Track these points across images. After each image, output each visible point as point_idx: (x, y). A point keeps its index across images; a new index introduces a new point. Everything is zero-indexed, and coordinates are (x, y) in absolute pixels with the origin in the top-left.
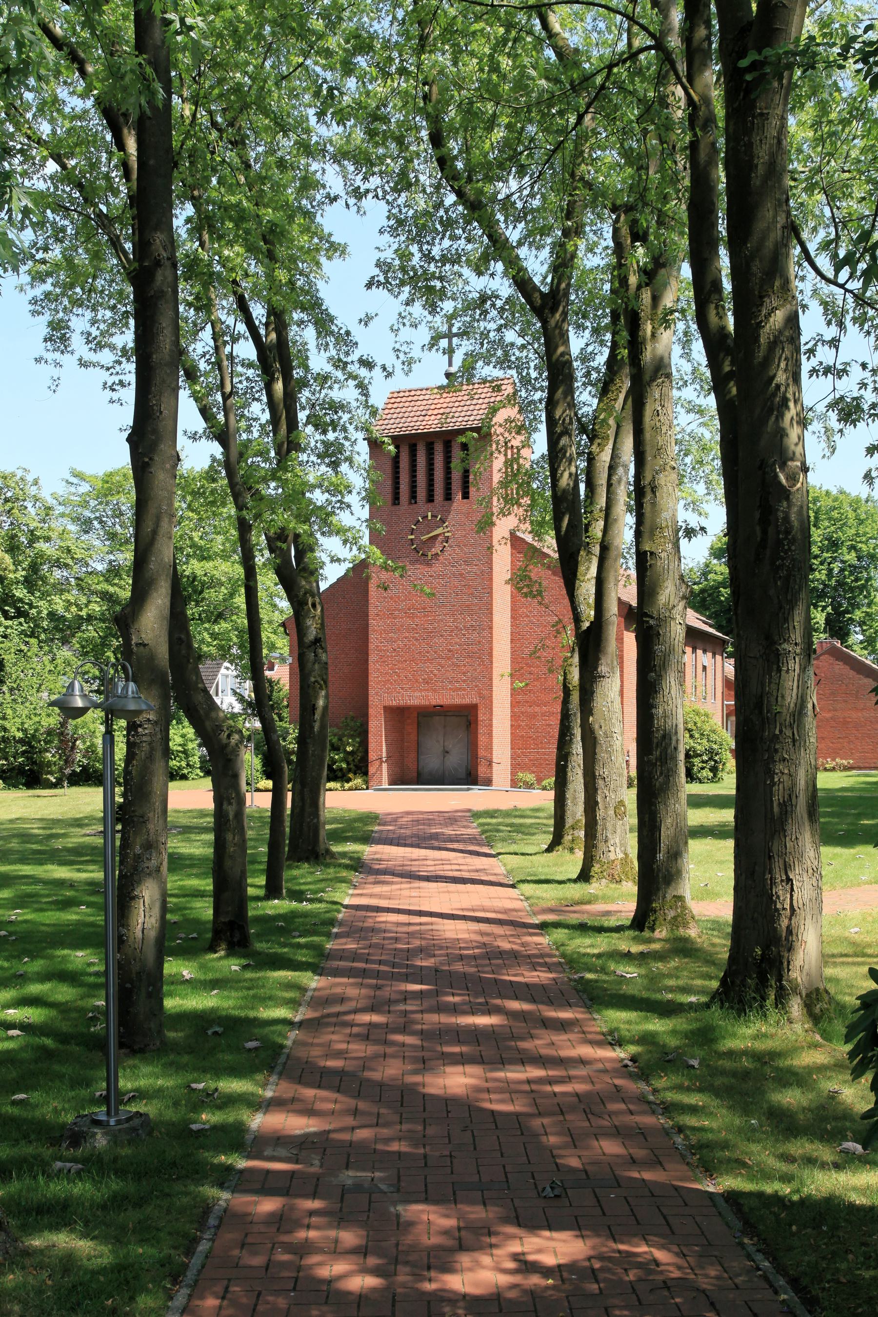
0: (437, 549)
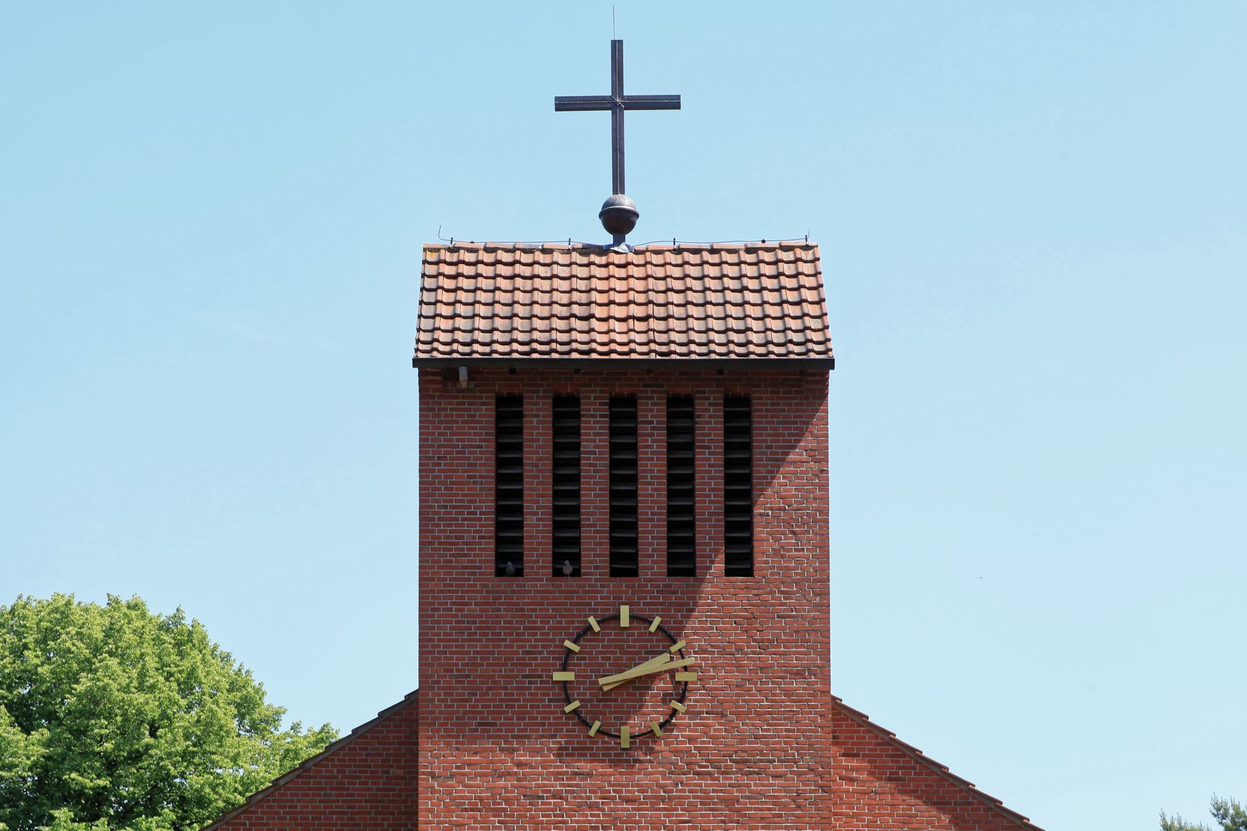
0: (650, 716)
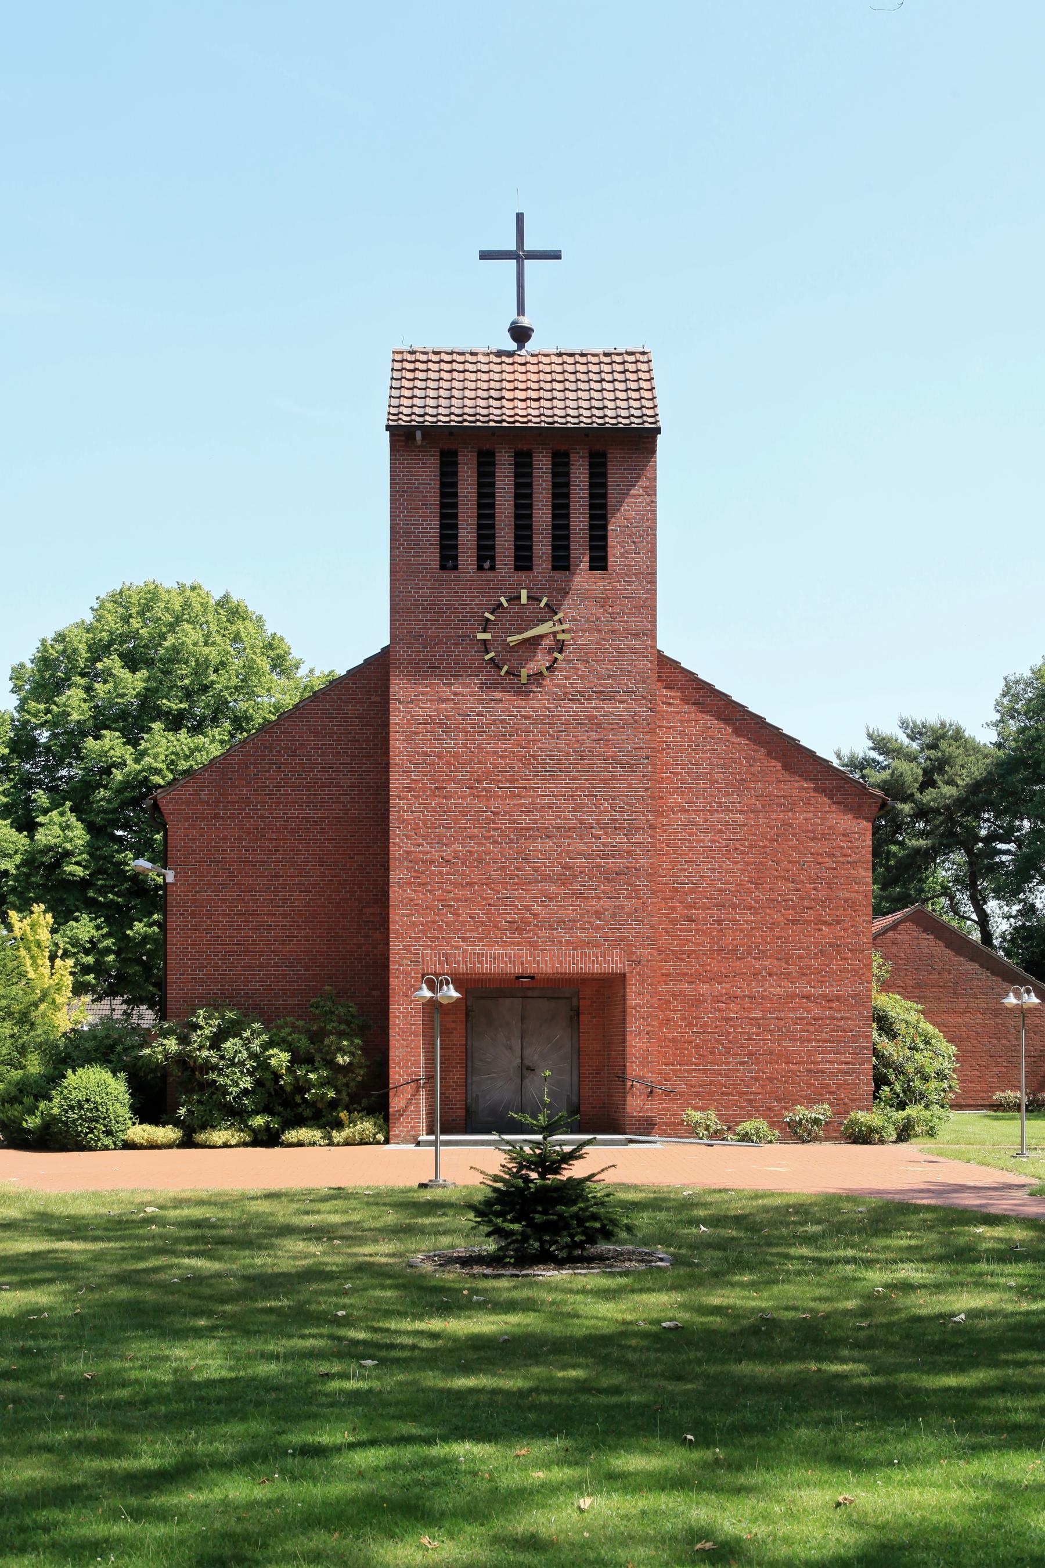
0: (539, 663)
